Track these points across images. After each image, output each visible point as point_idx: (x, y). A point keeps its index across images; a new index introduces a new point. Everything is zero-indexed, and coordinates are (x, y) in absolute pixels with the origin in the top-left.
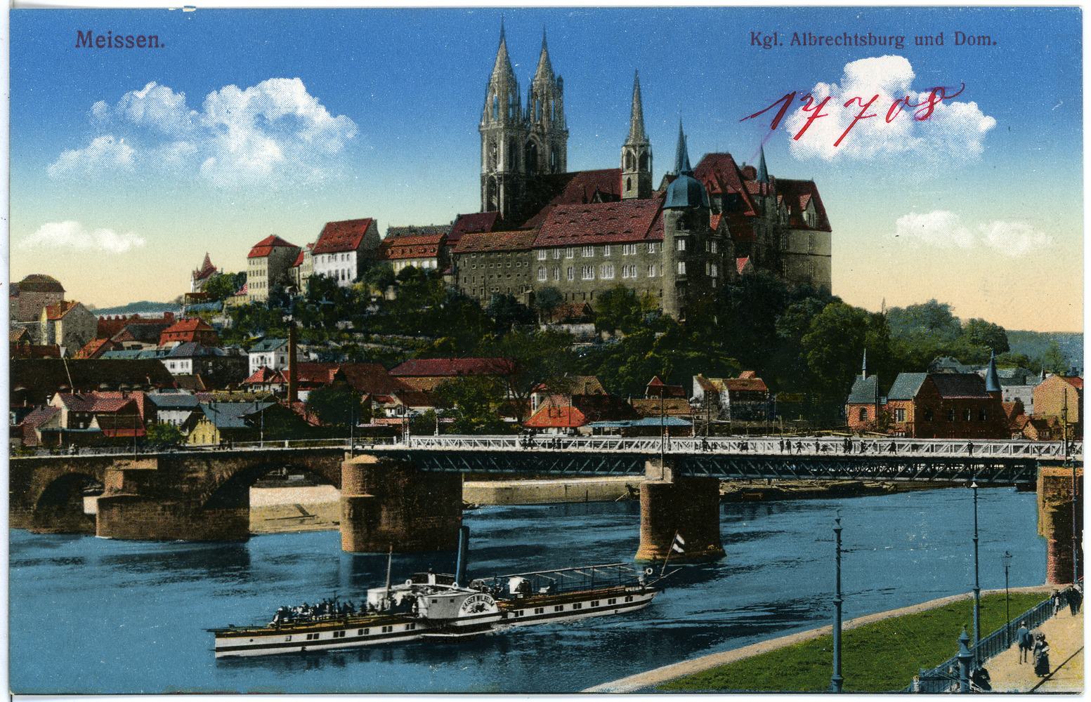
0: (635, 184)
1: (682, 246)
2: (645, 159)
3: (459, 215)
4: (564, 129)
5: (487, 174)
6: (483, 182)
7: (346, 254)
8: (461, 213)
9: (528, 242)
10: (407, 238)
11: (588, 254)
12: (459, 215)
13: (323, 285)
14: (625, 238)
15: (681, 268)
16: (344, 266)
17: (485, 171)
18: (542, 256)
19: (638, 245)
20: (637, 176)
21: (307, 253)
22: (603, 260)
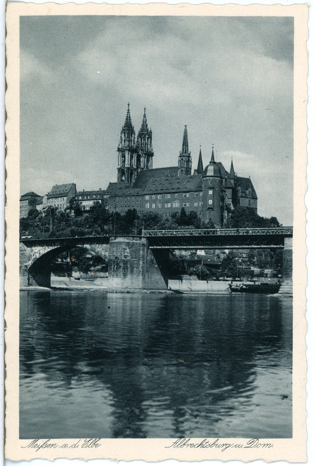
0: (184, 172)
1: (211, 192)
2: (189, 161)
3: (110, 183)
4: (152, 152)
5: (121, 168)
6: (119, 172)
7: (62, 198)
8: (112, 182)
9: (141, 193)
10: (87, 195)
11: (169, 196)
12: (110, 183)
13: (52, 211)
14: (185, 190)
15: (210, 202)
16: (62, 204)
17: (119, 167)
18: (147, 197)
19: (190, 193)
20: (185, 169)
21: (46, 197)
22: (175, 199)
